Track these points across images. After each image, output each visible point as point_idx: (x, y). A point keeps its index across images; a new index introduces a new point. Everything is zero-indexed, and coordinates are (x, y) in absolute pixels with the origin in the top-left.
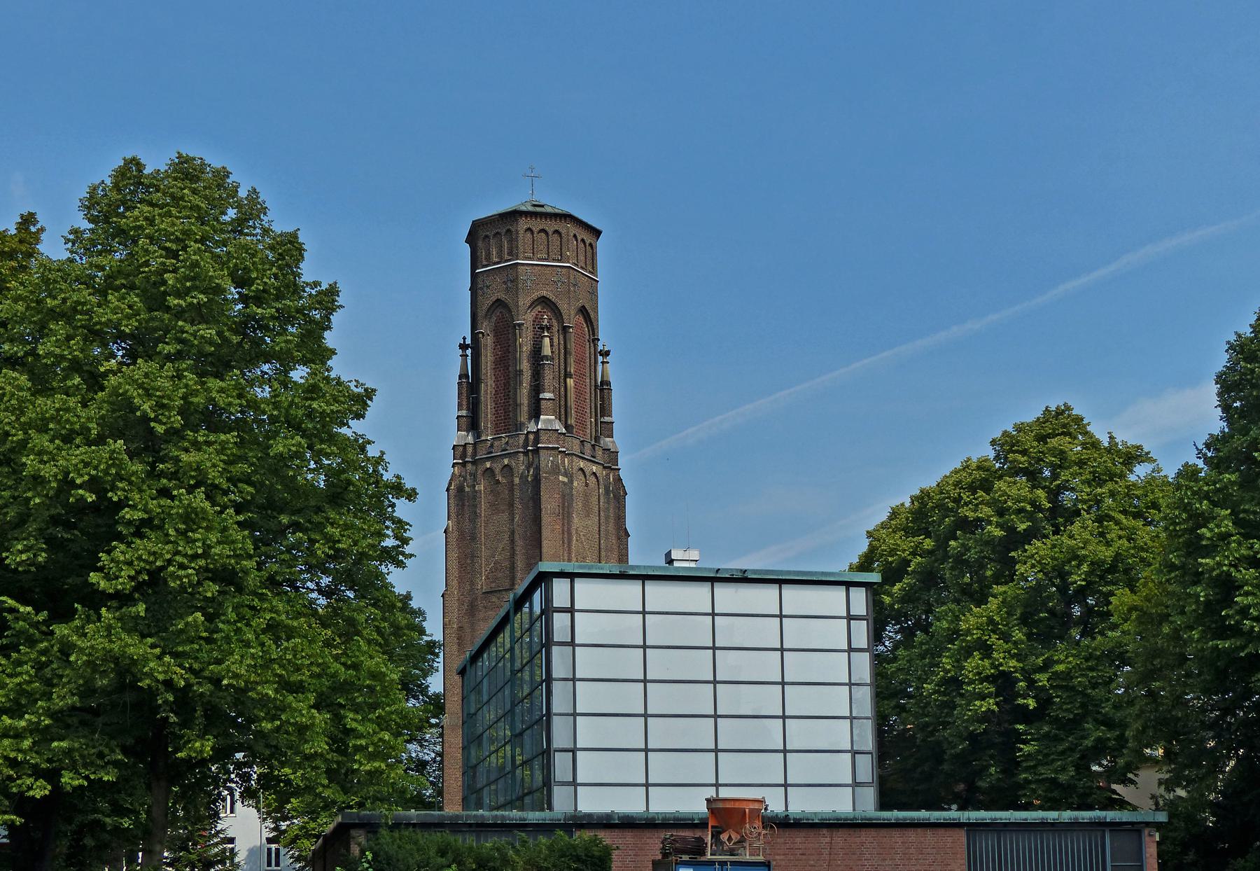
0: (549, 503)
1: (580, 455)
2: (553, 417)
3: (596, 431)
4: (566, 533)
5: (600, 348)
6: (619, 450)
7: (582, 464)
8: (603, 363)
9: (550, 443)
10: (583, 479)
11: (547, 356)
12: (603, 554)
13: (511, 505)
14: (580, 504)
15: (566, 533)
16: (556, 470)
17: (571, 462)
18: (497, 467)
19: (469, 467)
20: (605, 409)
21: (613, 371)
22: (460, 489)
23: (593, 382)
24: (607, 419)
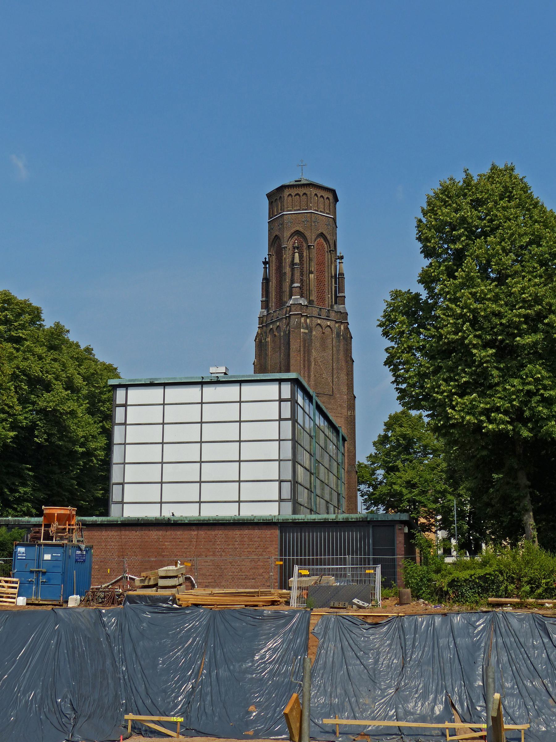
0: (295, 345)
1: (318, 316)
2: (299, 297)
3: (332, 302)
4: (306, 362)
5: (338, 254)
6: (348, 311)
7: (319, 322)
8: (339, 263)
9: (296, 311)
10: (321, 329)
11: (296, 263)
12: (335, 371)
13: (280, 348)
14: (318, 345)
15: (306, 362)
16: (299, 326)
17: (311, 321)
18: (275, 327)
19: (265, 328)
20: (340, 288)
21: (346, 267)
22: (260, 341)
23: (330, 274)
24: (341, 294)
